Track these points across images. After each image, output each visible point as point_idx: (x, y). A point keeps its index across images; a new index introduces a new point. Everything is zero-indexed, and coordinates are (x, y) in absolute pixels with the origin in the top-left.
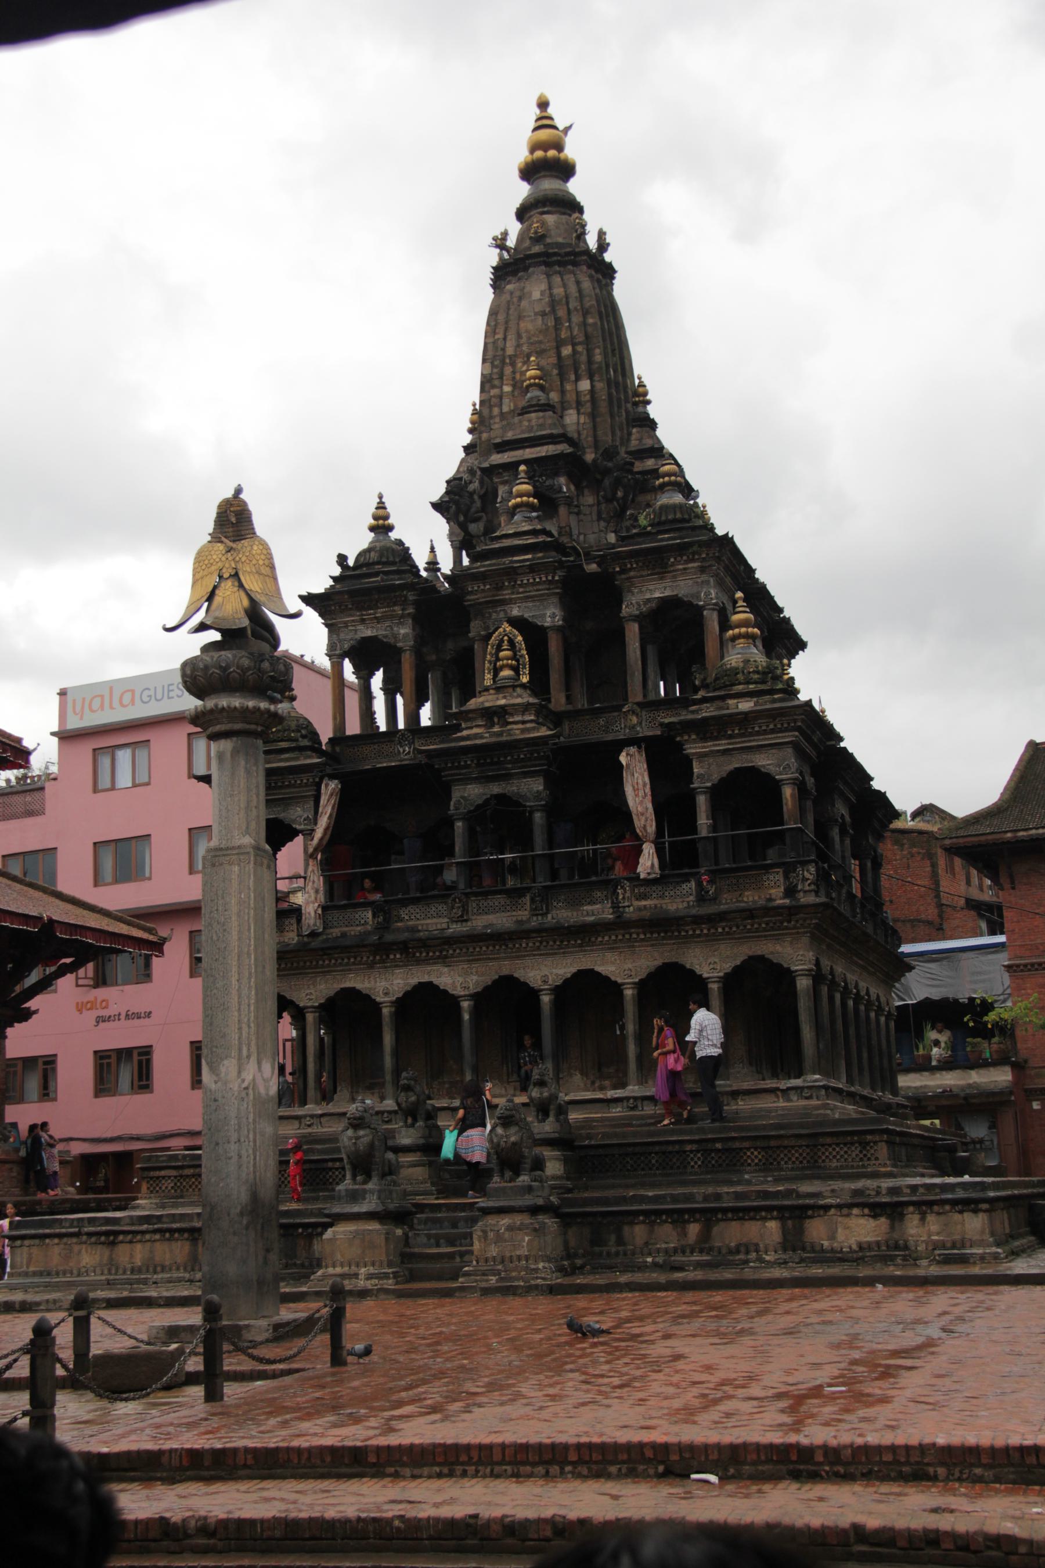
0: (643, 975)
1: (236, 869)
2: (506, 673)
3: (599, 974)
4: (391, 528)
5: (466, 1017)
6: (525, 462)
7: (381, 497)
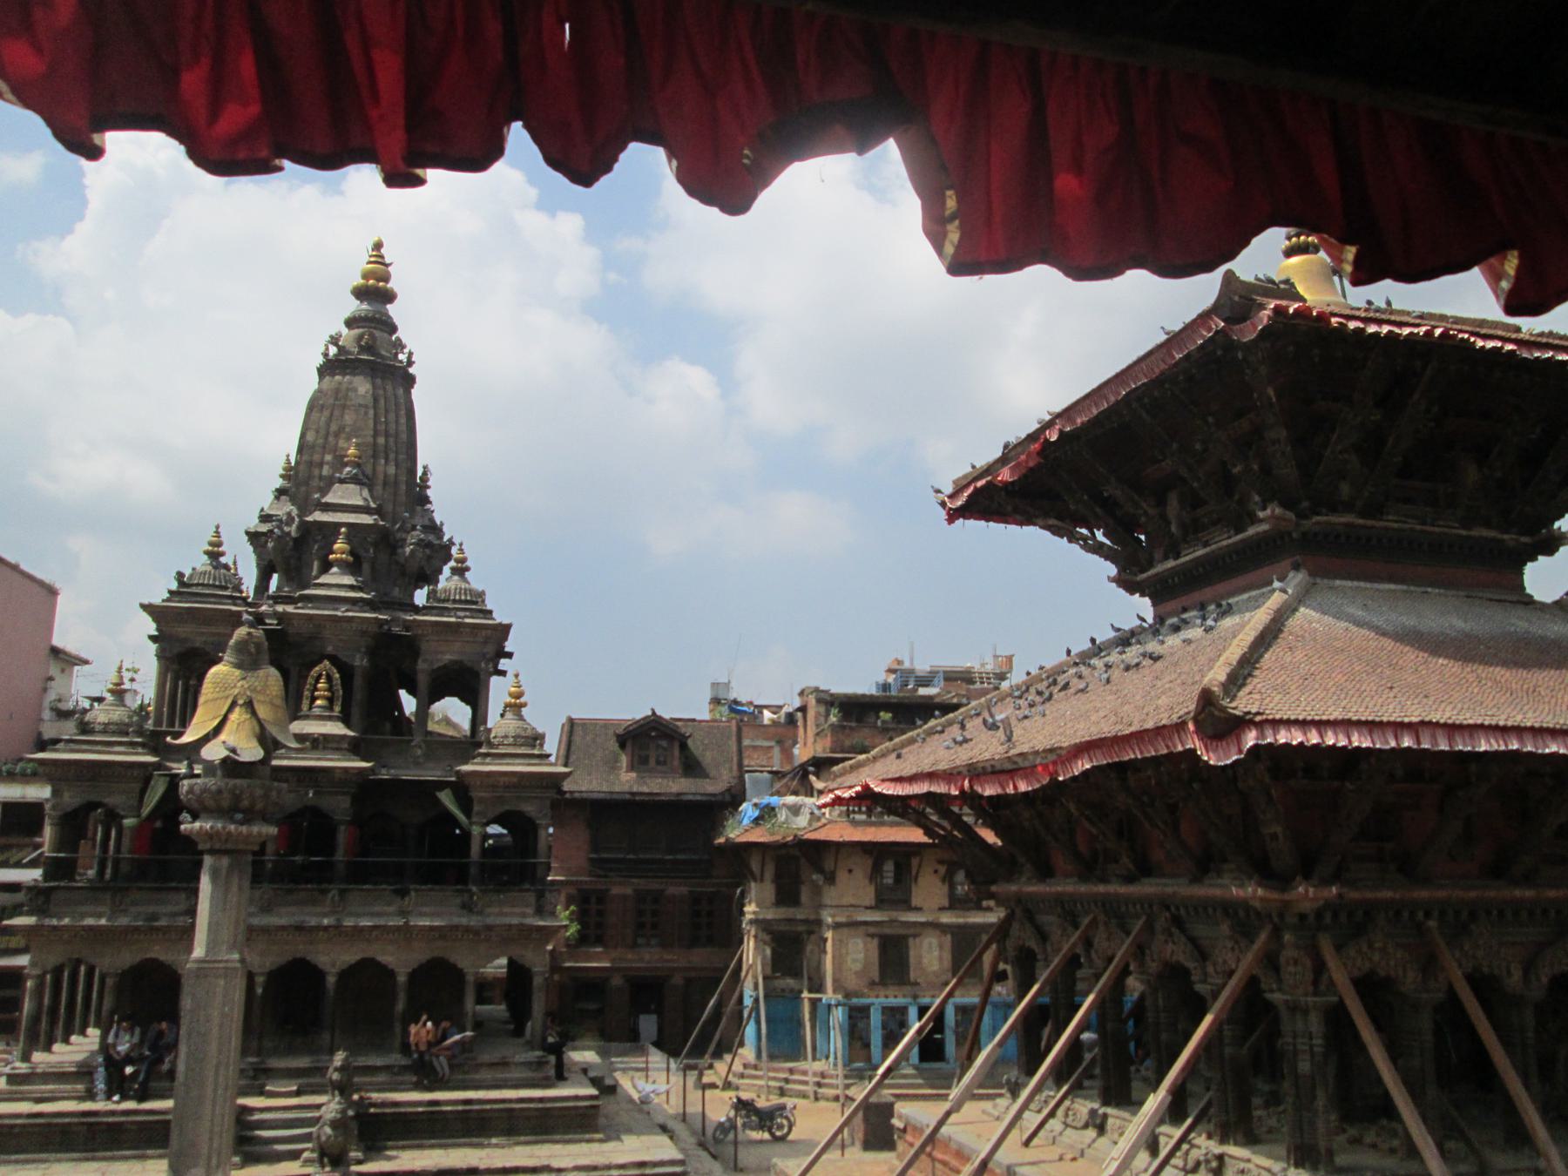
1: (222, 982)
2: (319, 702)
4: (223, 554)
6: (349, 525)
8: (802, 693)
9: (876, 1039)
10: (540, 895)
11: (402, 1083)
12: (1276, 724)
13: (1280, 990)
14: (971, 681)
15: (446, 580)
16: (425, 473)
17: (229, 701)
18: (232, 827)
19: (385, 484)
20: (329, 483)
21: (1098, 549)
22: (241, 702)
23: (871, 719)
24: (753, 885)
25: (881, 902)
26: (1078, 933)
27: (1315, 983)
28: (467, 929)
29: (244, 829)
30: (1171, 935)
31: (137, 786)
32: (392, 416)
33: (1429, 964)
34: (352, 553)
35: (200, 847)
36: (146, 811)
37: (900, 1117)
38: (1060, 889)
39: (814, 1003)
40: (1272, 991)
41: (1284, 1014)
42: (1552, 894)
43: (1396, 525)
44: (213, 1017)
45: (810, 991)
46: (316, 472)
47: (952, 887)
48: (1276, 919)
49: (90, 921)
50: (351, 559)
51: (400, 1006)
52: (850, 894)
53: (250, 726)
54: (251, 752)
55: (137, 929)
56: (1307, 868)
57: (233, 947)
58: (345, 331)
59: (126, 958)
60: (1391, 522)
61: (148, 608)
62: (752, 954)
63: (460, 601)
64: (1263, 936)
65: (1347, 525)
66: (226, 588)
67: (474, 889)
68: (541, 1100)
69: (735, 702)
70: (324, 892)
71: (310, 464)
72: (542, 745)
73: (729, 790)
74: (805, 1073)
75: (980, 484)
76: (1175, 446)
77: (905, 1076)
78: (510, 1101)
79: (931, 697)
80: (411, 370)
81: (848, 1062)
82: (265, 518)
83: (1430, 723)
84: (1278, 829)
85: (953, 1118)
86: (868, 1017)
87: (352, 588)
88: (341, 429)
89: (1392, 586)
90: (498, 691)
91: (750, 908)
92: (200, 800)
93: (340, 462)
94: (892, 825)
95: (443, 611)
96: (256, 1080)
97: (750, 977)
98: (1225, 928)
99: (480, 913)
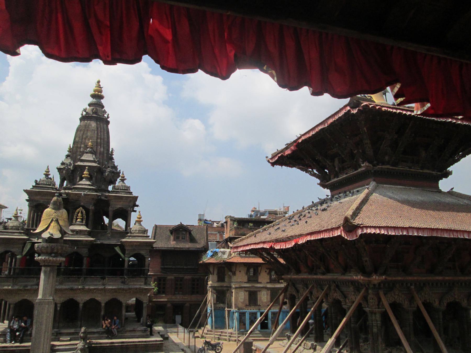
0: (107, 300)
1: (47, 306)
2: (78, 220)
3: (96, 300)
4: (50, 175)
6: (89, 166)
7: (48, 166)
8: (226, 218)
9: (247, 322)
10: (146, 279)
11: (103, 337)
12: (367, 227)
13: (368, 307)
14: (276, 214)
15: (118, 183)
16: (112, 151)
17: (51, 220)
18: (51, 258)
19: (100, 154)
20: (82, 153)
21: (314, 175)
22: (54, 220)
23: (246, 225)
24: (211, 275)
25: (249, 281)
26: (308, 290)
27: (378, 305)
28: (123, 289)
29: (55, 259)
30: (336, 291)
31: (22, 246)
32: (102, 133)
33: (412, 299)
34: (89, 174)
35: (41, 264)
36: (24, 253)
37: (254, 346)
38: (303, 277)
39: (229, 311)
40: (365, 307)
41: (369, 315)
42: (447, 278)
43: (402, 169)
44: (44, 317)
45: (228, 308)
46: (79, 150)
47: (270, 277)
48: (367, 286)
49: (6, 287)
50: (89, 176)
51: (102, 313)
52: (240, 278)
53: (57, 227)
54: (57, 235)
55: (21, 290)
56: (376, 271)
57: (50, 296)
58: (88, 107)
59: (17, 299)
60: (400, 168)
61: (26, 191)
62: (210, 297)
63: (123, 189)
64: (363, 291)
65: (388, 168)
66: (50, 185)
67: (126, 277)
68: (145, 342)
69: (206, 220)
70: (79, 278)
71: (77, 147)
72: (147, 233)
73: (204, 247)
74: (226, 333)
75: (279, 155)
76: (337, 145)
77: (256, 334)
78: (136, 342)
79: (264, 219)
80: (108, 119)
81: (239, 329)
82: (63, 164)
83: (412, 227)
84: (367, 259)
85: (271, 346)
86: (245, 316)
87: (89, 185)
88: (87, 137)
89: (401, 187)
90: (134, 217)
91: (210, 283)
92: (41, 250)
93: (86, 147)
94: (253, 257)
95: (117, 192)
96: (57, 336)
97: (209, 304)
98: (352, 288)
99: (127, 284)
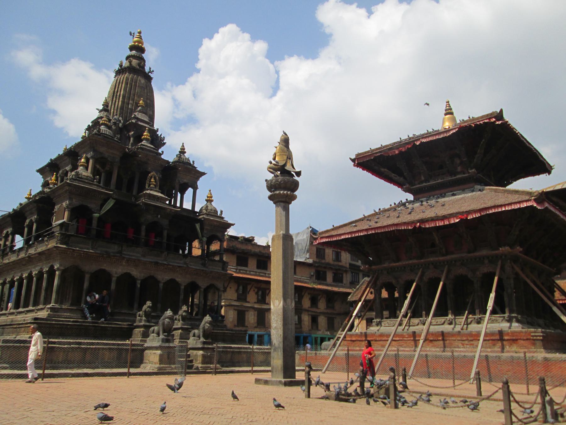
2: (152, 186)
5: (139, 286)
20: (132, 111)
25: (239, 299)
36: (103, 212)
47: (258, 297)
93: (137, 105)
99: (207, 267)
